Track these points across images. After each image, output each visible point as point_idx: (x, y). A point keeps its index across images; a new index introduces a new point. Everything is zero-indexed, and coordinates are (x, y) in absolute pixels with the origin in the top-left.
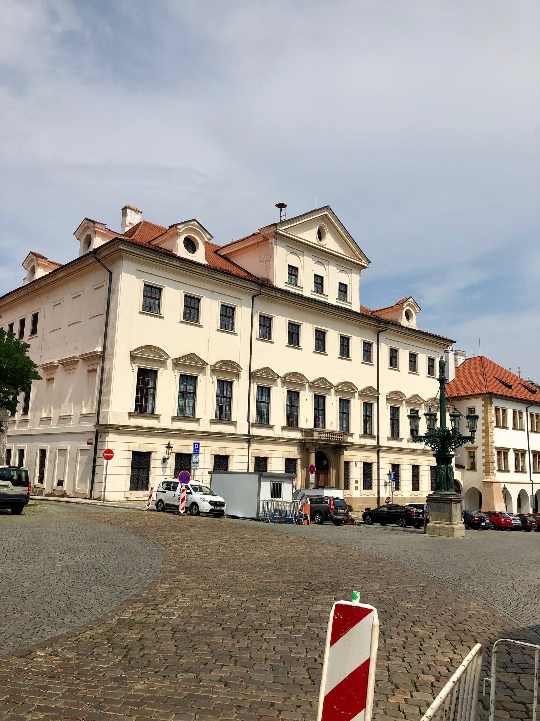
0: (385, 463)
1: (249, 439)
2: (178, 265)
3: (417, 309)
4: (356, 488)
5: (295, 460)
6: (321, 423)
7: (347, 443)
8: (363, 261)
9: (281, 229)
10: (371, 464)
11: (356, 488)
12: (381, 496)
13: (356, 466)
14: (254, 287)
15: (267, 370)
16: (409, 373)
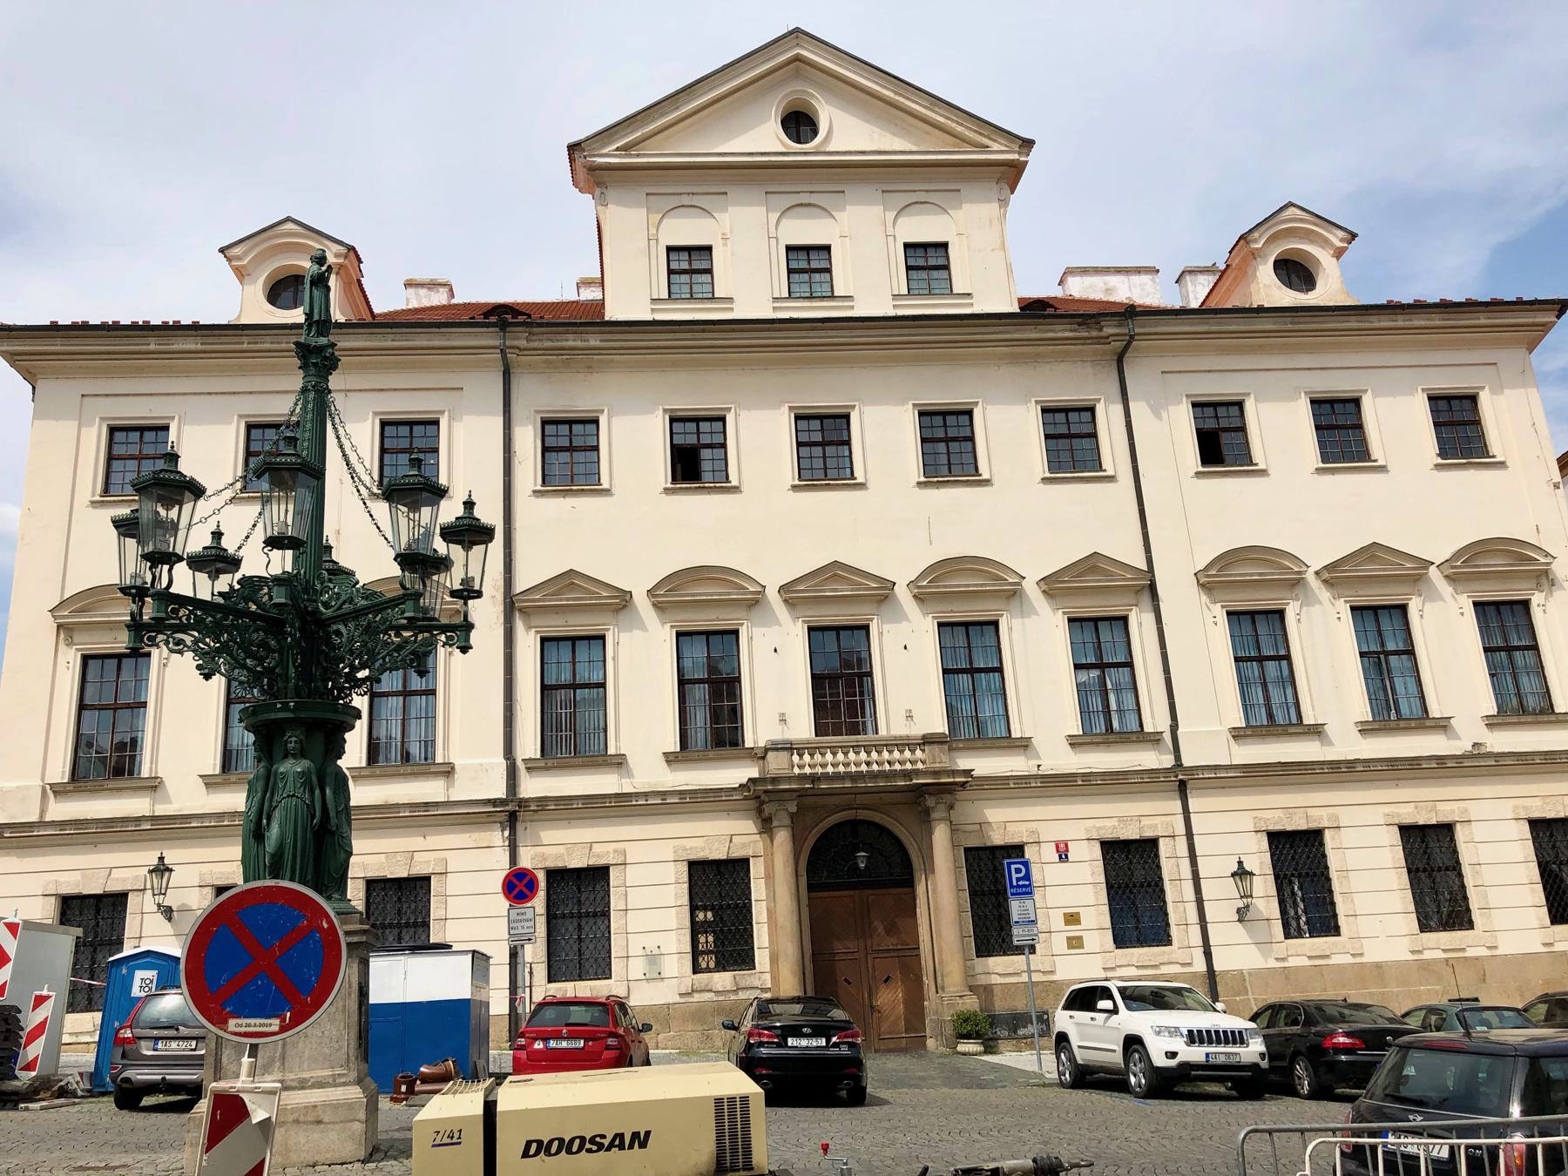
1: (511, 814)
2: (192, 347)
3: (1336, 238)
4: (1075, 943)
5: (744, 863)
7: (954, 773)
8: (996, 147)
9: (605, 151)
10: (1151, 844)
11: (1075, 943)
12: (1217, 967)
13: (1063, 856)
14: (490, 338)
15: (569, 580)
16: (1319, 471)
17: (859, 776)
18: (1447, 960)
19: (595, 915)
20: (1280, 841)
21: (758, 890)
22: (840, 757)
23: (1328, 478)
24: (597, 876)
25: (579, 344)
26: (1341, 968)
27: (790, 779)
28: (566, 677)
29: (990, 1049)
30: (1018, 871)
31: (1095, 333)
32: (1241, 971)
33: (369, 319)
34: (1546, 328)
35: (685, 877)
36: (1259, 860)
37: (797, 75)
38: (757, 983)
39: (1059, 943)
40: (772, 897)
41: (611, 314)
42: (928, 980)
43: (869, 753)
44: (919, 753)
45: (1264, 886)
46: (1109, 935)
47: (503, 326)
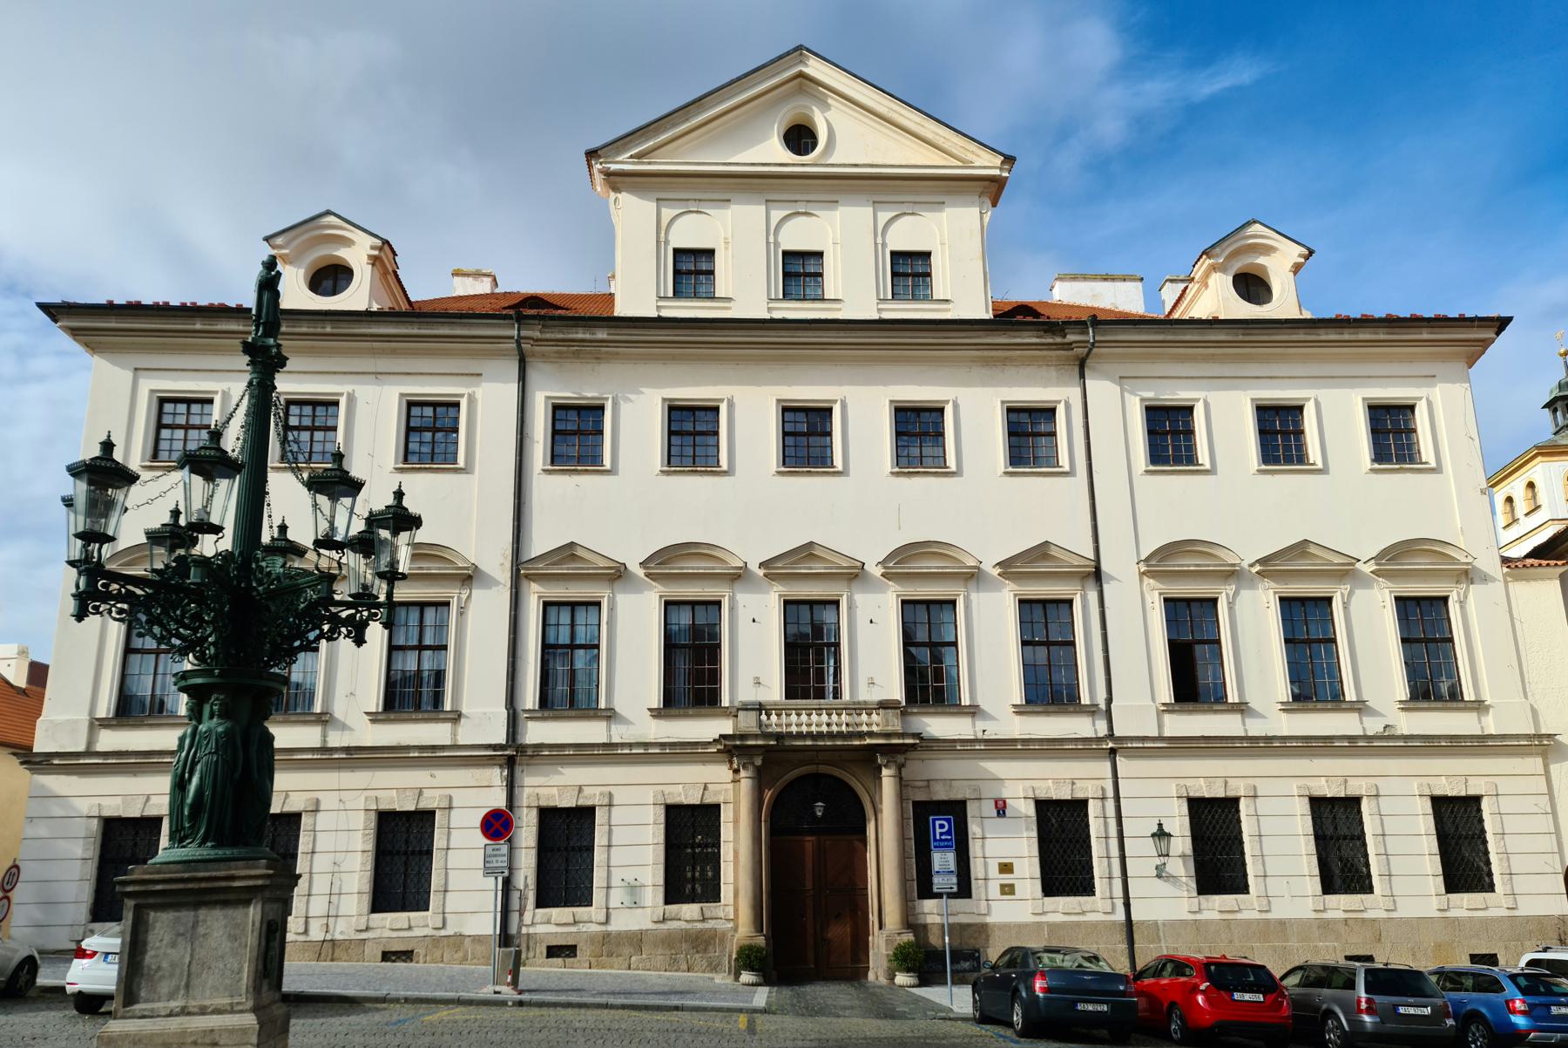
0: (1155, 799)
1: (513, 756)
6: (830, 684)
9: (620, 159)
11: (1008, 890)
12: (1134, 917)
15: (568, 552)
17: (820, 735)
18: (1346, 920)
19: (580, 849)
20: (1197, 807)
21: (726, 831)
22: (804, 718)
23: (1268, 477)
24: (585, 814)
25: (588, 336)
26: (1249, 922)
27: (756, 736)
28: (564, 638)
29: (924, 982)
30: (942, 826)
31: (1059, 340)
32: (1156, 923)
33: (404, 307)
34: (1486, 344)
35: (662, 819)
36: (1179, 825)
37: (801, 90)
38: (722, 915)
39: (994, 890)
40: (736, 840)
41: (621, 310)
42: (873, 918)
43: (829, 715)
44: (874, 716)
45: (1182, 843)
46: (1038, 885)
47: (521, 319)
